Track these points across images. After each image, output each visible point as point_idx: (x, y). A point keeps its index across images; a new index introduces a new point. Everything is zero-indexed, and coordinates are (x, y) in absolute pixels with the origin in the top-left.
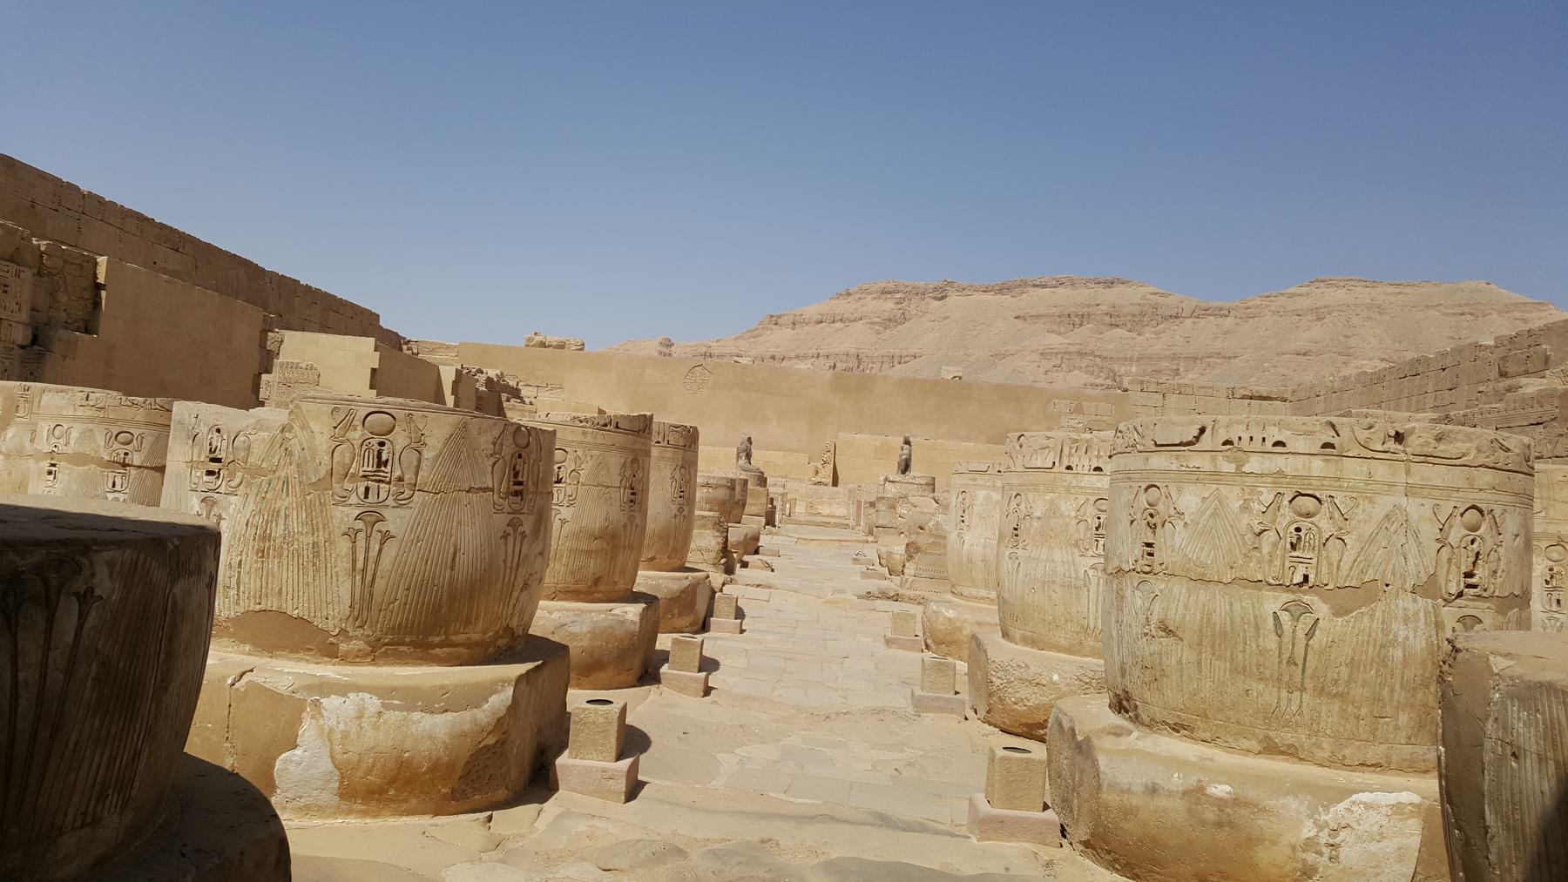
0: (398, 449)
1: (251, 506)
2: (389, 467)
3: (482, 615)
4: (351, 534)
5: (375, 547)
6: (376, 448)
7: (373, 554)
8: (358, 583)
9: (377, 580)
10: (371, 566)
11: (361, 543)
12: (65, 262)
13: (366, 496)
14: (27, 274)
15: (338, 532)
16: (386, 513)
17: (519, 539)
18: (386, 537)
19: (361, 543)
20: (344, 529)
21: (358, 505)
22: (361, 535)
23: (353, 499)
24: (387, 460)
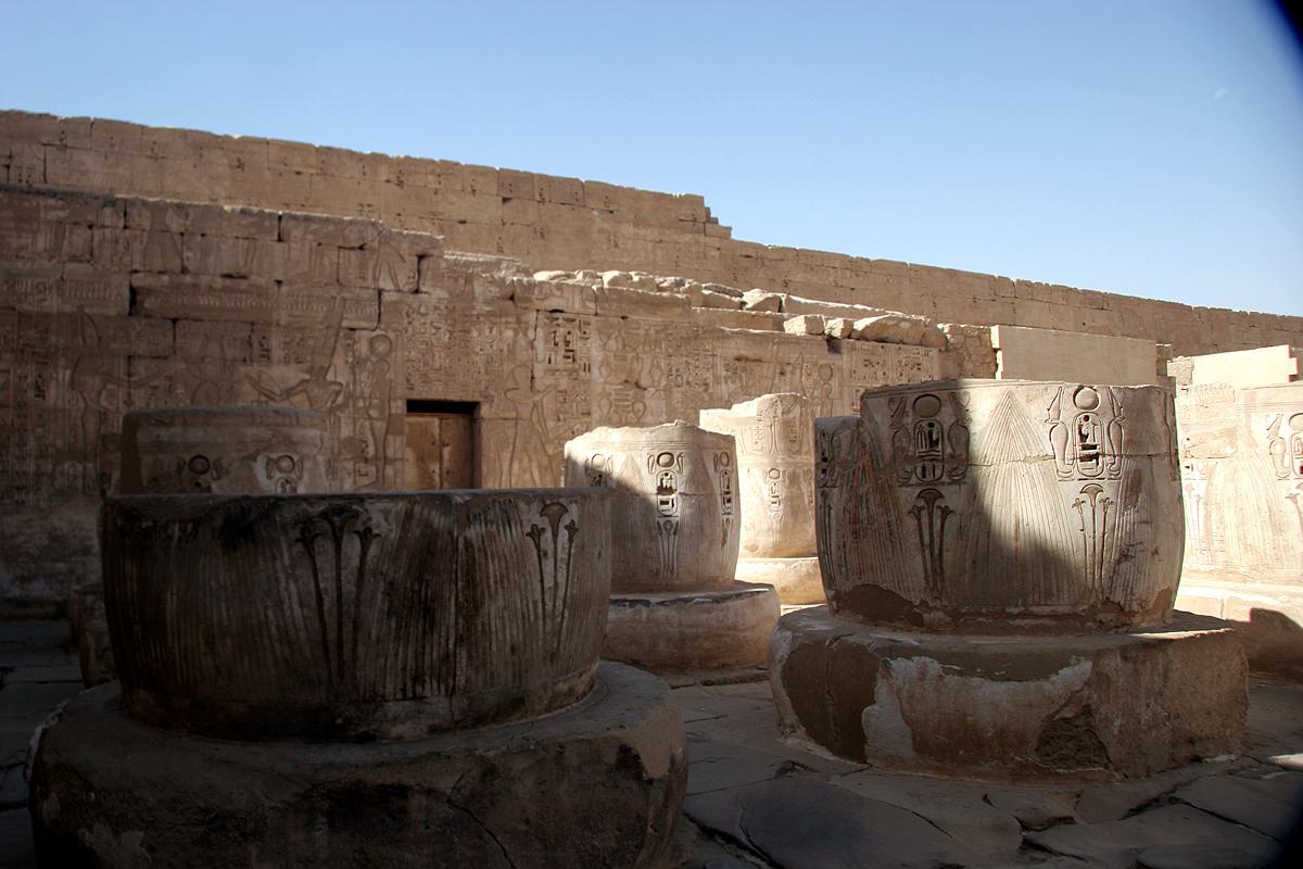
0: (946, 427)
1: (845, 495)
2: (940, 446)
3: (1066, 587)
4: (916, 512)
5: (937, 523)
6: (927, 429)
7: (937, 528)
8: (928, 557)
9: (945, 553)
10: (937, 540)
11: (925, 520)
12: (965, 338)
13: (924, 476)
14: (934, 353)
15: (905, 511)
16: (944, 490)
17: (1099, 507)
18: (946, 512)
19: (925, 520)
20: (909, 507)
21: (918, 485)
22: (924, 513)
23: (914, 480)
24: (938, 440)
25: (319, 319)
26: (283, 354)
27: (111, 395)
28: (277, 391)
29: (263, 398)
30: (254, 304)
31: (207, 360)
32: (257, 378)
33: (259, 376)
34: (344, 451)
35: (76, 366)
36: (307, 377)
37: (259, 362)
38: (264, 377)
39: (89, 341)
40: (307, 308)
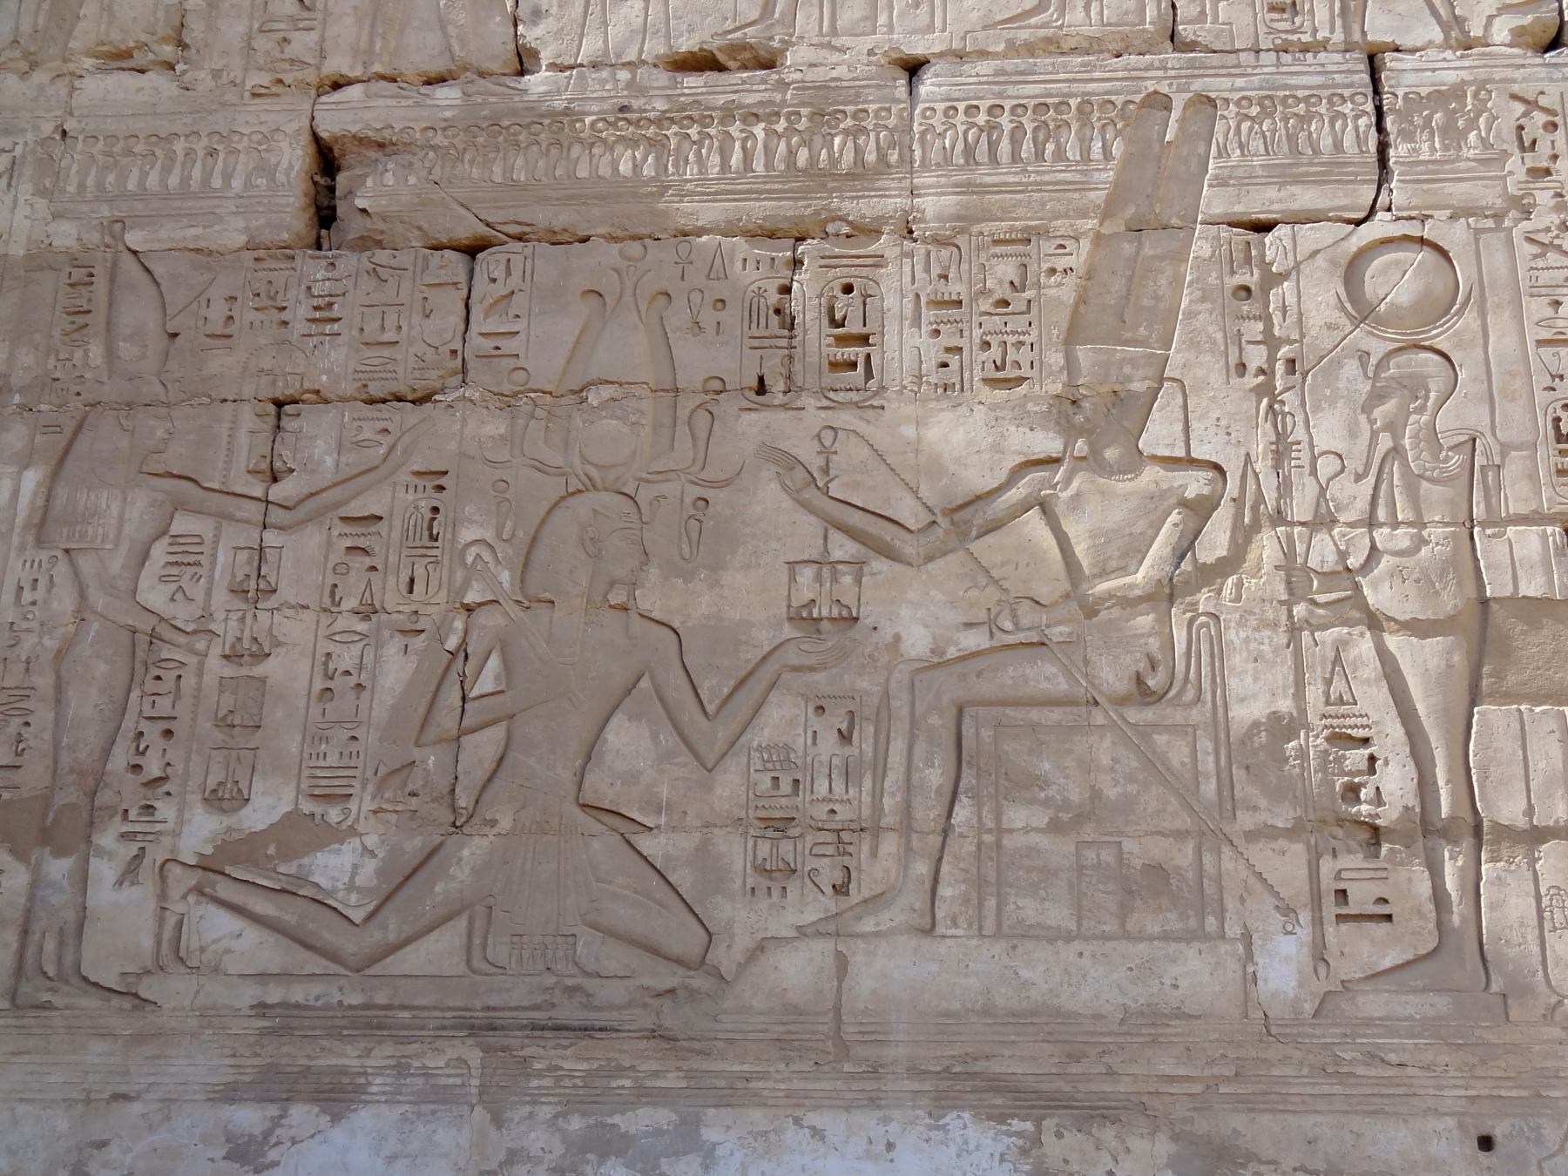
25: (1098, 196)
26: (932, 355)
27: (187, 559)
28: (907, 510)
29: (842, 548)
30: (803, 157)
31: (593, 398)
32: (815, 463)
33: (826, 452)
34: (1244, 788)
35: (61, 461)
36: (1047, 443)
37: (823, 392)
38: (850, 453)
39: (125, 349)
40: (1039, 155)
